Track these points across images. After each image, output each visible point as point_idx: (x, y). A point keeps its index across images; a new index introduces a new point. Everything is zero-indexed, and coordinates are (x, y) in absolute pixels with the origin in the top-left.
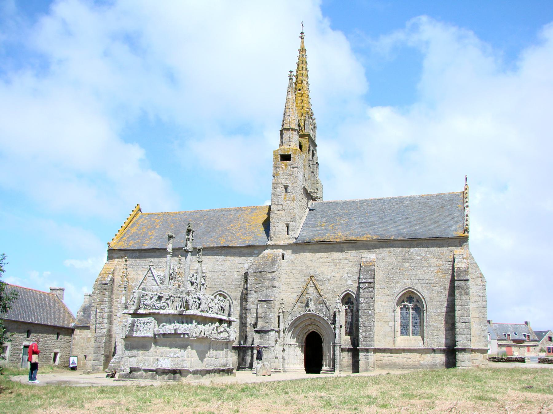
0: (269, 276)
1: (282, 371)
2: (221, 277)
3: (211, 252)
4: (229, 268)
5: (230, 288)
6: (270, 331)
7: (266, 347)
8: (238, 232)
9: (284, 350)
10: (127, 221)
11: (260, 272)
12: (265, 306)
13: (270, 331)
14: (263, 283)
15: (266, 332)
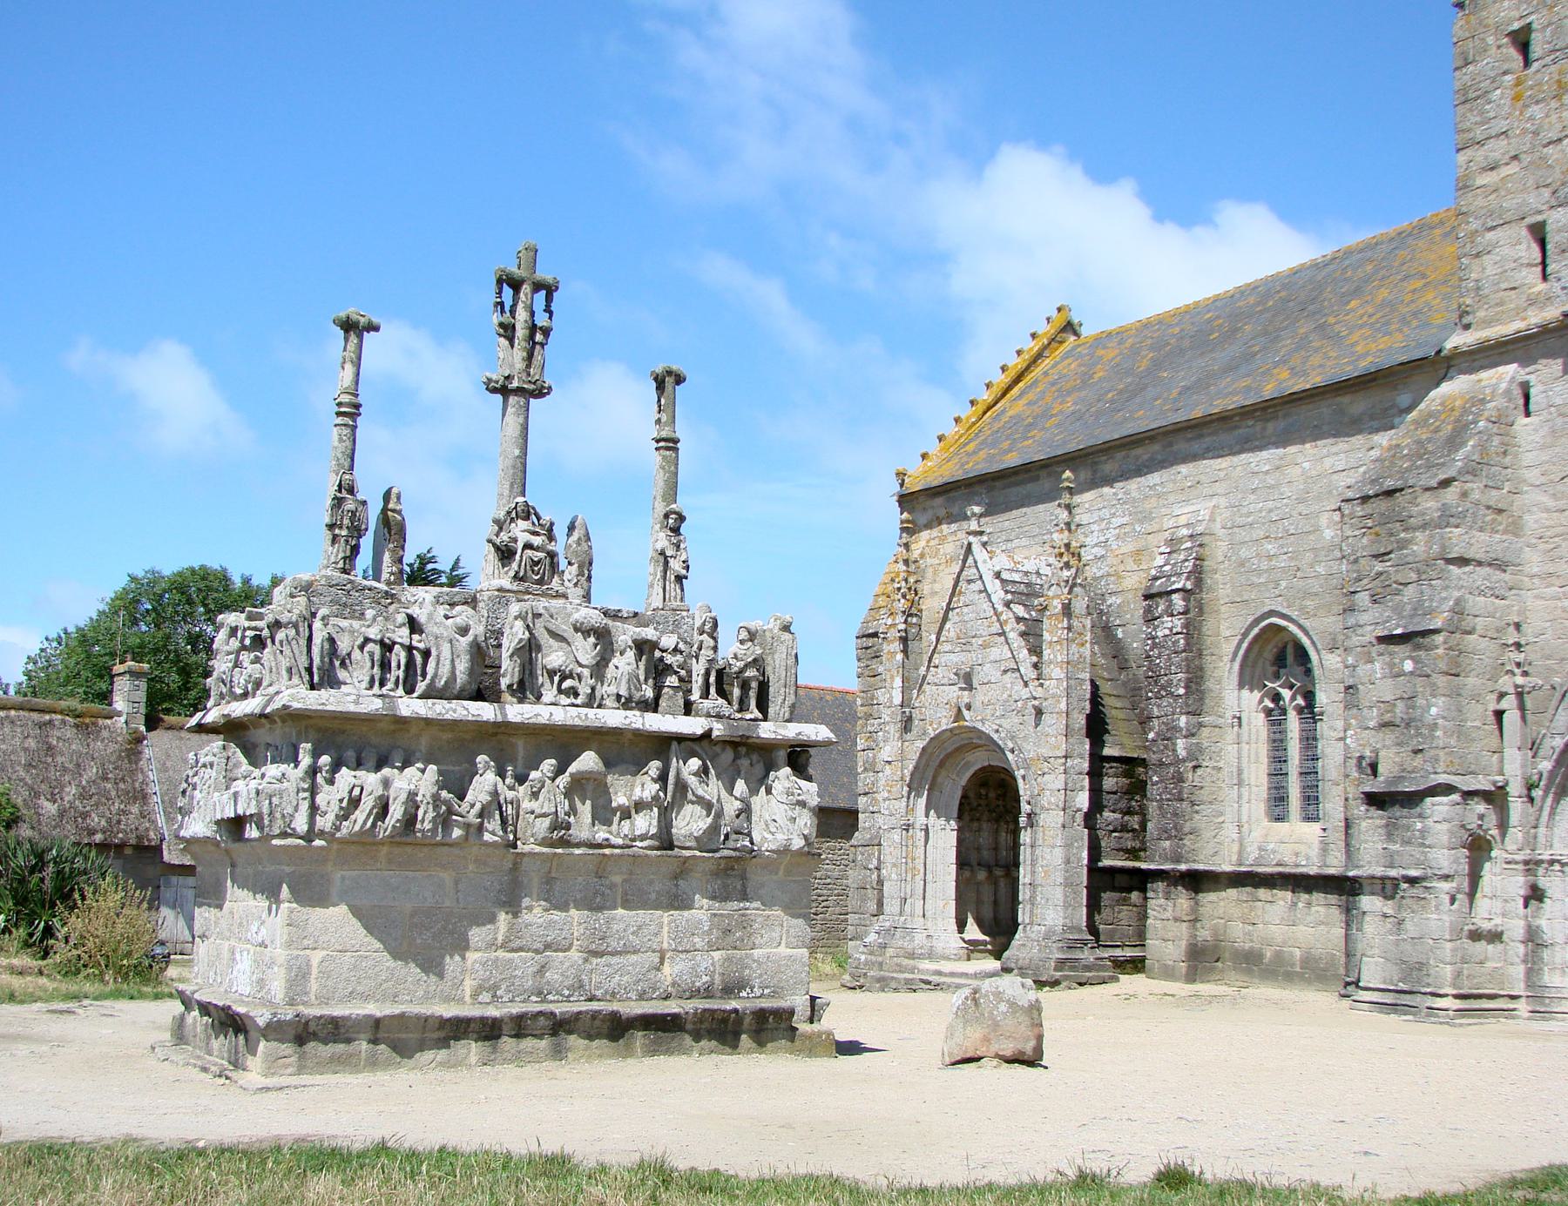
0: (1429, 505)
1: (1522, 1007)
2: (1270, 547)
3: (1225, 438)
4: (1301, 501)
5: (1308, 594)
6: (1434, 791)
7: (1413, 881)
8: (1361, 327)
9: (1535, 895)
10: (1001, 379)
11: (1390, 493)
12: (1408, 666)
13: (1434, 791)
14: (1403, 544)
15: (1412, 799)
